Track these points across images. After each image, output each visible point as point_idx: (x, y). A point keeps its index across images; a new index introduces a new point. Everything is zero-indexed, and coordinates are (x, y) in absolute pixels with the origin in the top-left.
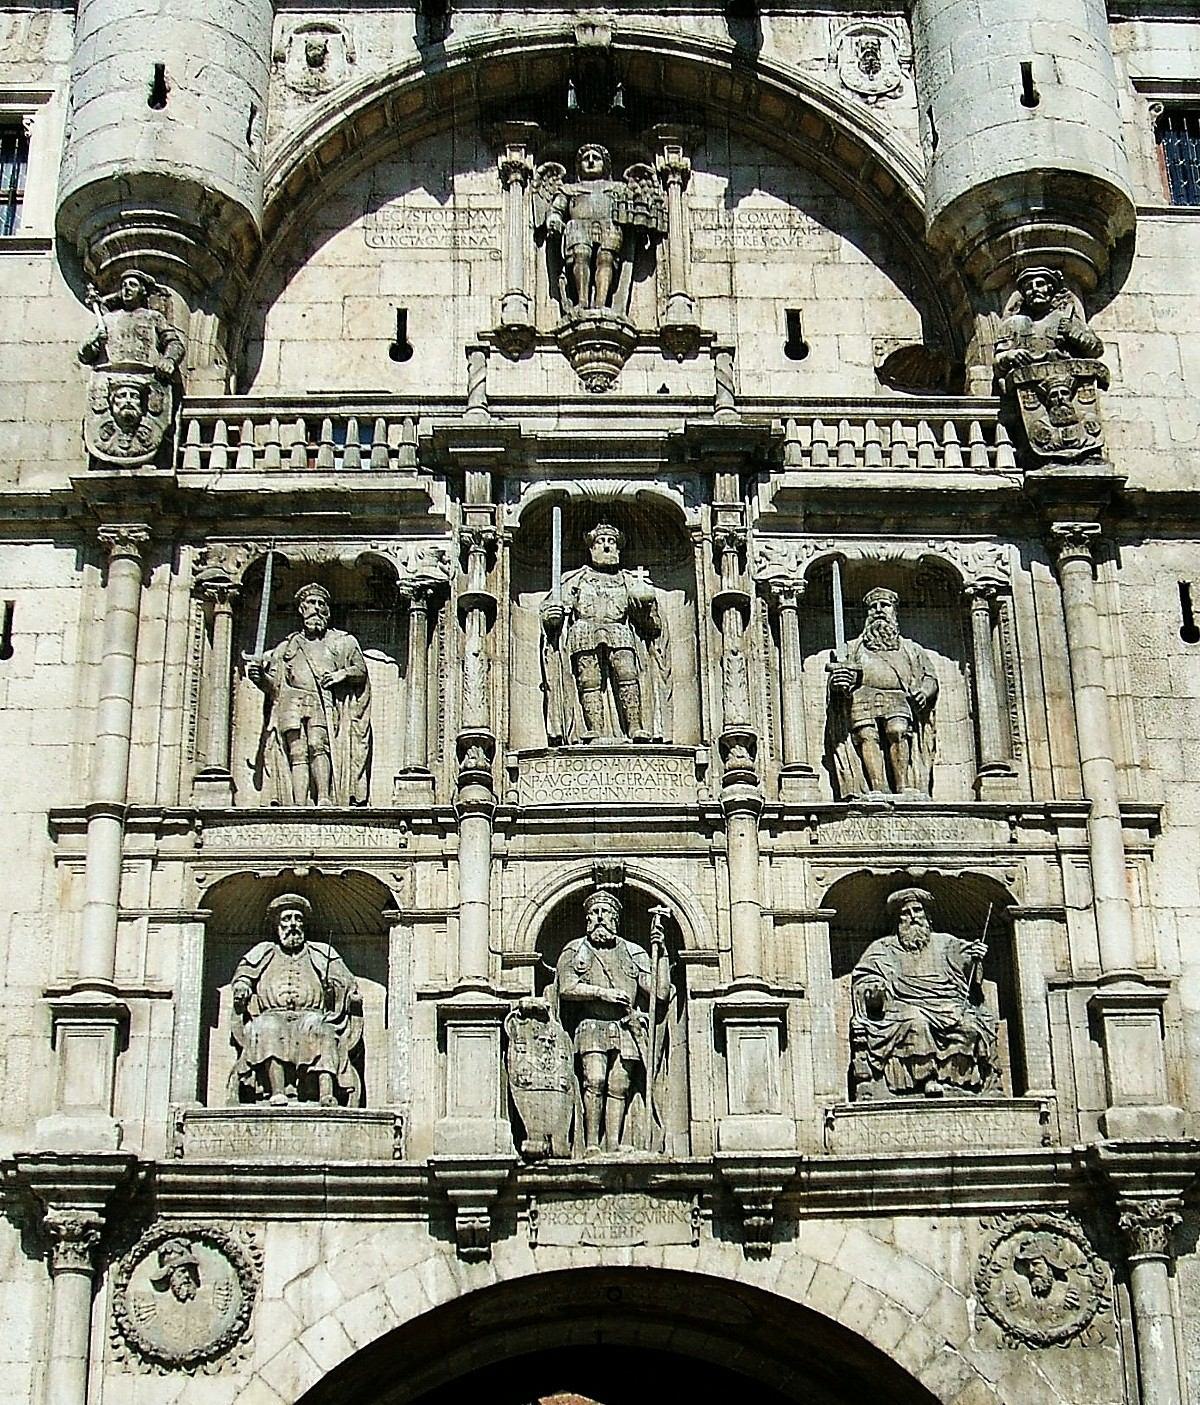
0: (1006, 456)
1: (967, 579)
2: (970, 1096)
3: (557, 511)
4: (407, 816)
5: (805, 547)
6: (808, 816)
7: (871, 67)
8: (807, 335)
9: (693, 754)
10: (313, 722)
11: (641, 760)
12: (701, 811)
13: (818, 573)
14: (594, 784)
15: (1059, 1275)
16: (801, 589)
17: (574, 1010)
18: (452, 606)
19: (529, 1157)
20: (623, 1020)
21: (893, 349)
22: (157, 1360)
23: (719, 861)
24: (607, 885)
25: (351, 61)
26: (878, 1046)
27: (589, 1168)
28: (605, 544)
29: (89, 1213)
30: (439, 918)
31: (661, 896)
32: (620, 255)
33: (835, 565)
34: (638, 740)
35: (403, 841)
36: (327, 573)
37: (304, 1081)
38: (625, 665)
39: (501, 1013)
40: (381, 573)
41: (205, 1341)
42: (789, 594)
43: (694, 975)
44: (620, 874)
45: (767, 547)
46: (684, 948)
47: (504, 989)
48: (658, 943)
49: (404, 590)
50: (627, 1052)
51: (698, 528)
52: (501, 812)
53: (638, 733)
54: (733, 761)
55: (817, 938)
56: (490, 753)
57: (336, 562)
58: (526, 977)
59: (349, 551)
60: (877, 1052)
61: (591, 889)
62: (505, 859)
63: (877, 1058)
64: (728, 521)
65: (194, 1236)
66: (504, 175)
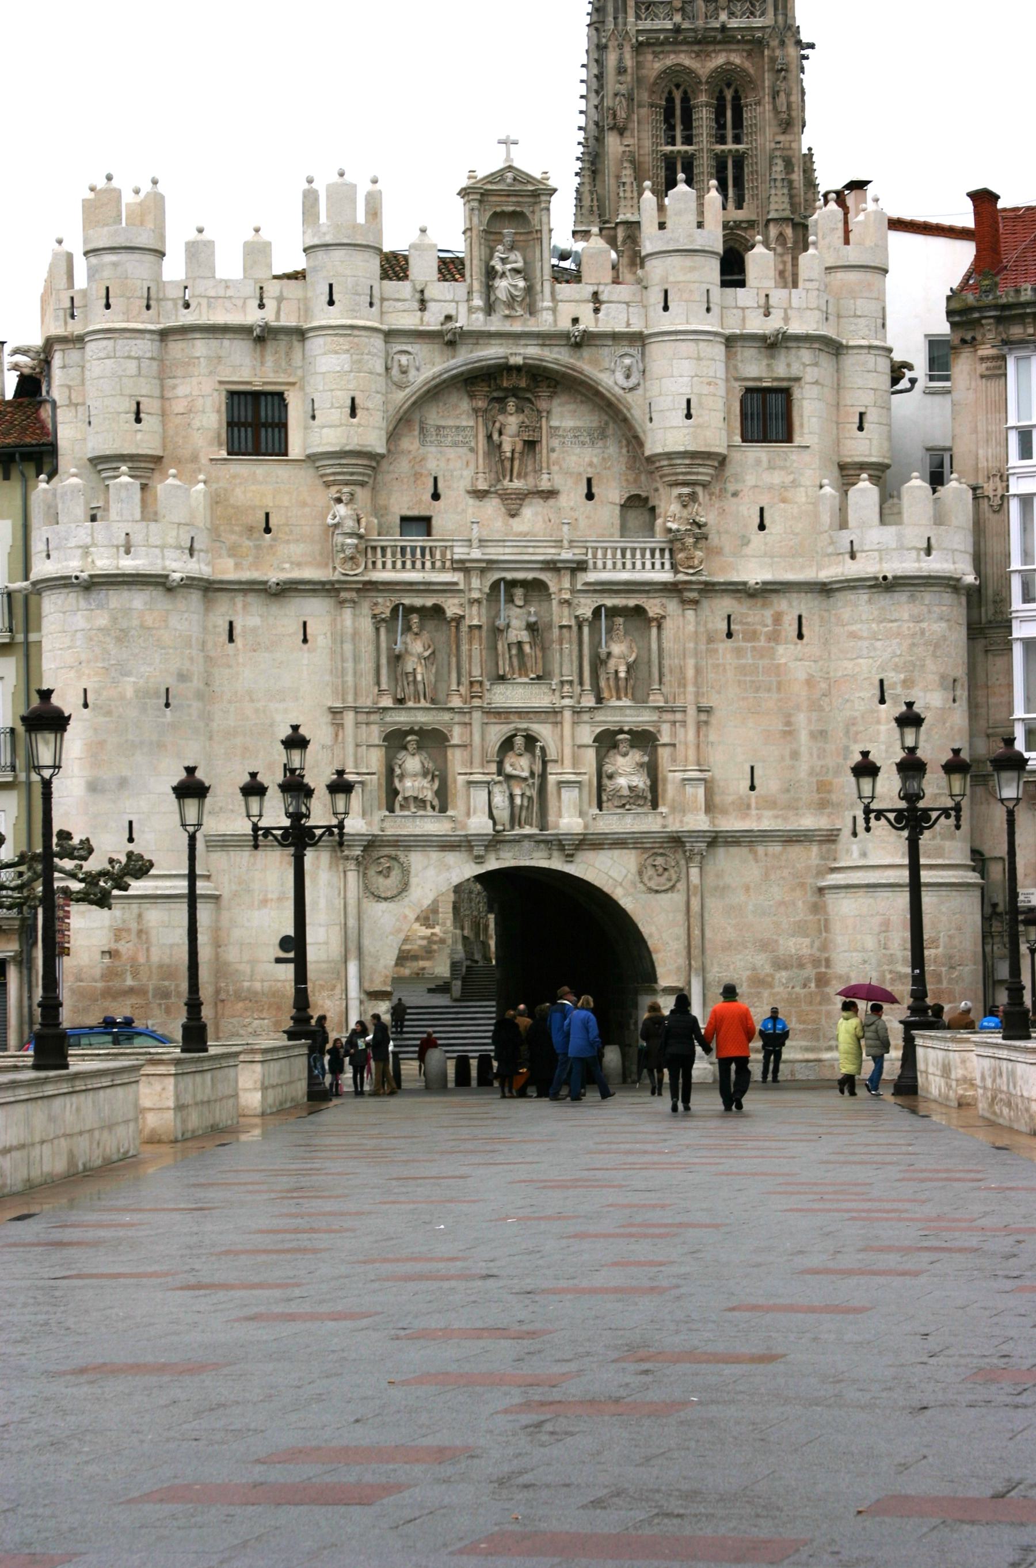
0: (667, 566)
1: (651, 614)
2: (640, 810)
7: (628, 377)
8: (594, 490)
10: (419, 670)
13: (597, 612)
15: (665, 869)
17: (509, 777)
21: (627, 495)
22: (379, 898)
25: (418, 369)
28: (519, 592)
29: (357, 852)
32: (522, 453)
36: (421, 611)
37: (421, 803)
38: (527, 648)
39: (488, 783)
40: (438, 611)
41: (395, 892)
43: (551, 768)
44: (525, 730)
50: (528, 793)
53: (533, 676)
55: (590, 755)
56: (481, 683)
58: (493, 768)
59: (429, 602)
61: (515, 735)
64: (567, 596)
65: (389, 857)
66: (476, 411)
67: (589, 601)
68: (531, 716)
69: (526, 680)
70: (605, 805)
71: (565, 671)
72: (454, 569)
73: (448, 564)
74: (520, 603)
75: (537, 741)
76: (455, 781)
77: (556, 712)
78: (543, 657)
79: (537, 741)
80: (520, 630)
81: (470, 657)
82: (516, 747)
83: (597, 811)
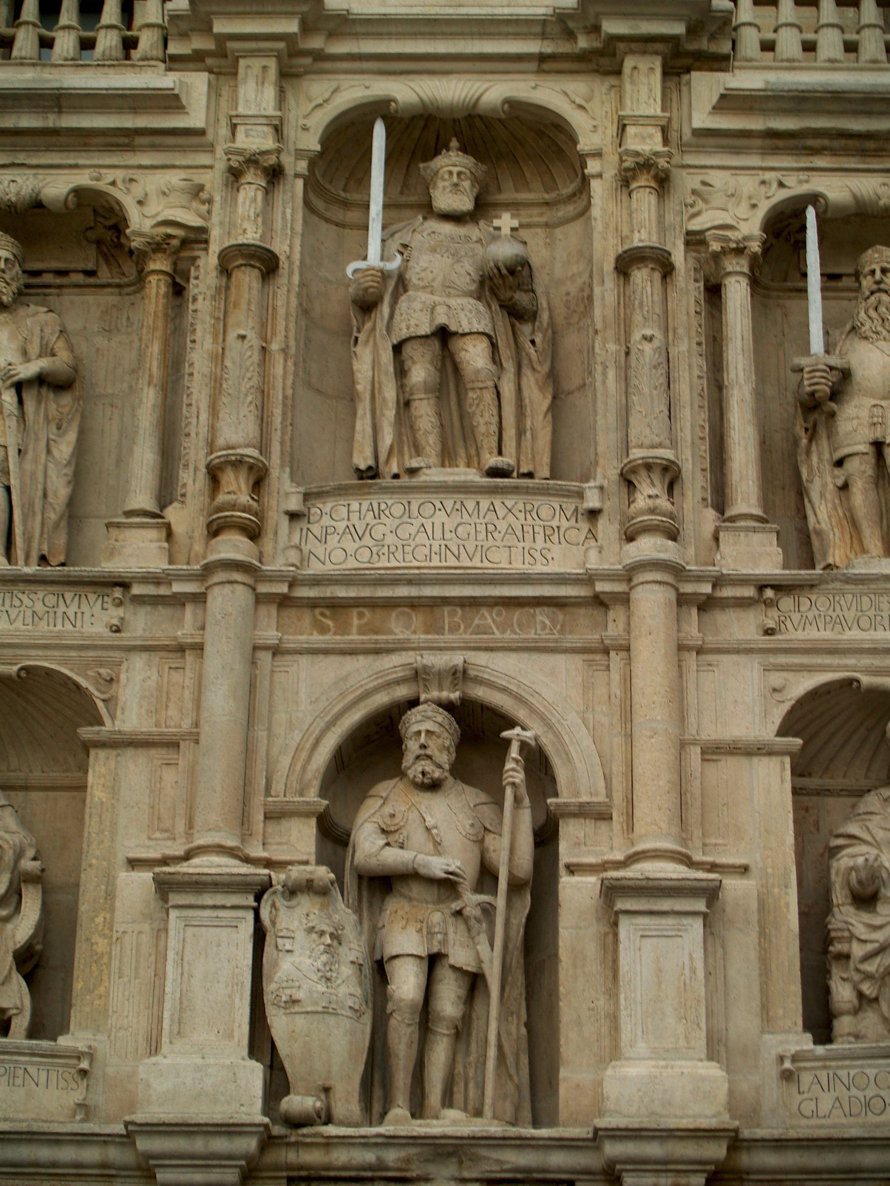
3: (379, 131)
4: (125, 585)
5: (763, 182)
6: (761, 588)
9: (580, 495)
11: (498, 504)
12: (589, 579)
14: (422, 538)
16: (755, 247)
18: (209, 261)
19: (296, 1123)
20: (456, 906)
23: (616, 658)
24: (435, 694)
26: (868, 957)
27: (391, 1141)
30: (172, 744)
31: (521, 714)
33: (811, 214)
34: (495, 472)
35: (115, 621)
39: (260, 891)
42: (739, 251)
44: (460, 675)
45: (704, 183)
46: (556, 795)
47: (265, 854)
48: (513, 784)
49: (136, 243)
51: (598, 154)
52: (271, 578)
53: (493, 460)
54: (641, 502)
57: (37, 205)
60: (871, 967)
61: (414, 703)
62: (277, 651)
63: (868, 977)
67: (748, 184)
68: (487, 617)
69: (473, 476)
70: (843, 1024)
71: (639, 429)
72: (173, 62)
73: (147, 41)
74: (464, 203)
75: (511, 723)
76: (110, 895)
77: (600, 602)
78: (555, 408)
79: (511, 723)
80: (448, 288)
81: (216, 384)
82: (412, 747)
83: (805, 1043)
